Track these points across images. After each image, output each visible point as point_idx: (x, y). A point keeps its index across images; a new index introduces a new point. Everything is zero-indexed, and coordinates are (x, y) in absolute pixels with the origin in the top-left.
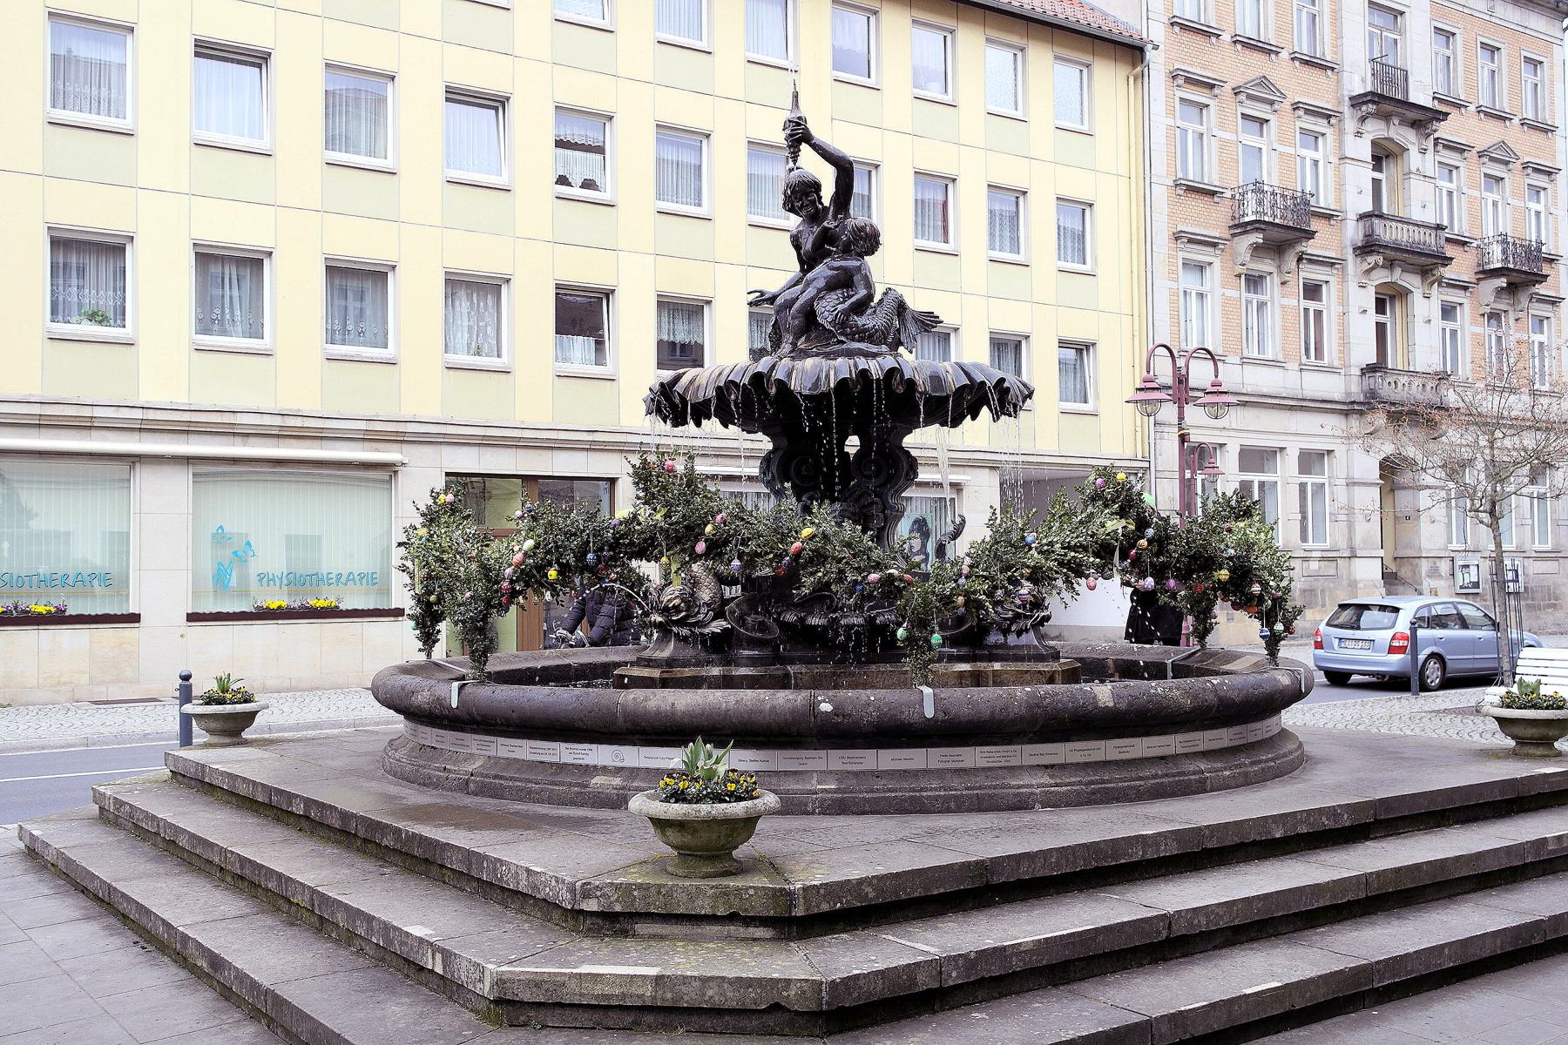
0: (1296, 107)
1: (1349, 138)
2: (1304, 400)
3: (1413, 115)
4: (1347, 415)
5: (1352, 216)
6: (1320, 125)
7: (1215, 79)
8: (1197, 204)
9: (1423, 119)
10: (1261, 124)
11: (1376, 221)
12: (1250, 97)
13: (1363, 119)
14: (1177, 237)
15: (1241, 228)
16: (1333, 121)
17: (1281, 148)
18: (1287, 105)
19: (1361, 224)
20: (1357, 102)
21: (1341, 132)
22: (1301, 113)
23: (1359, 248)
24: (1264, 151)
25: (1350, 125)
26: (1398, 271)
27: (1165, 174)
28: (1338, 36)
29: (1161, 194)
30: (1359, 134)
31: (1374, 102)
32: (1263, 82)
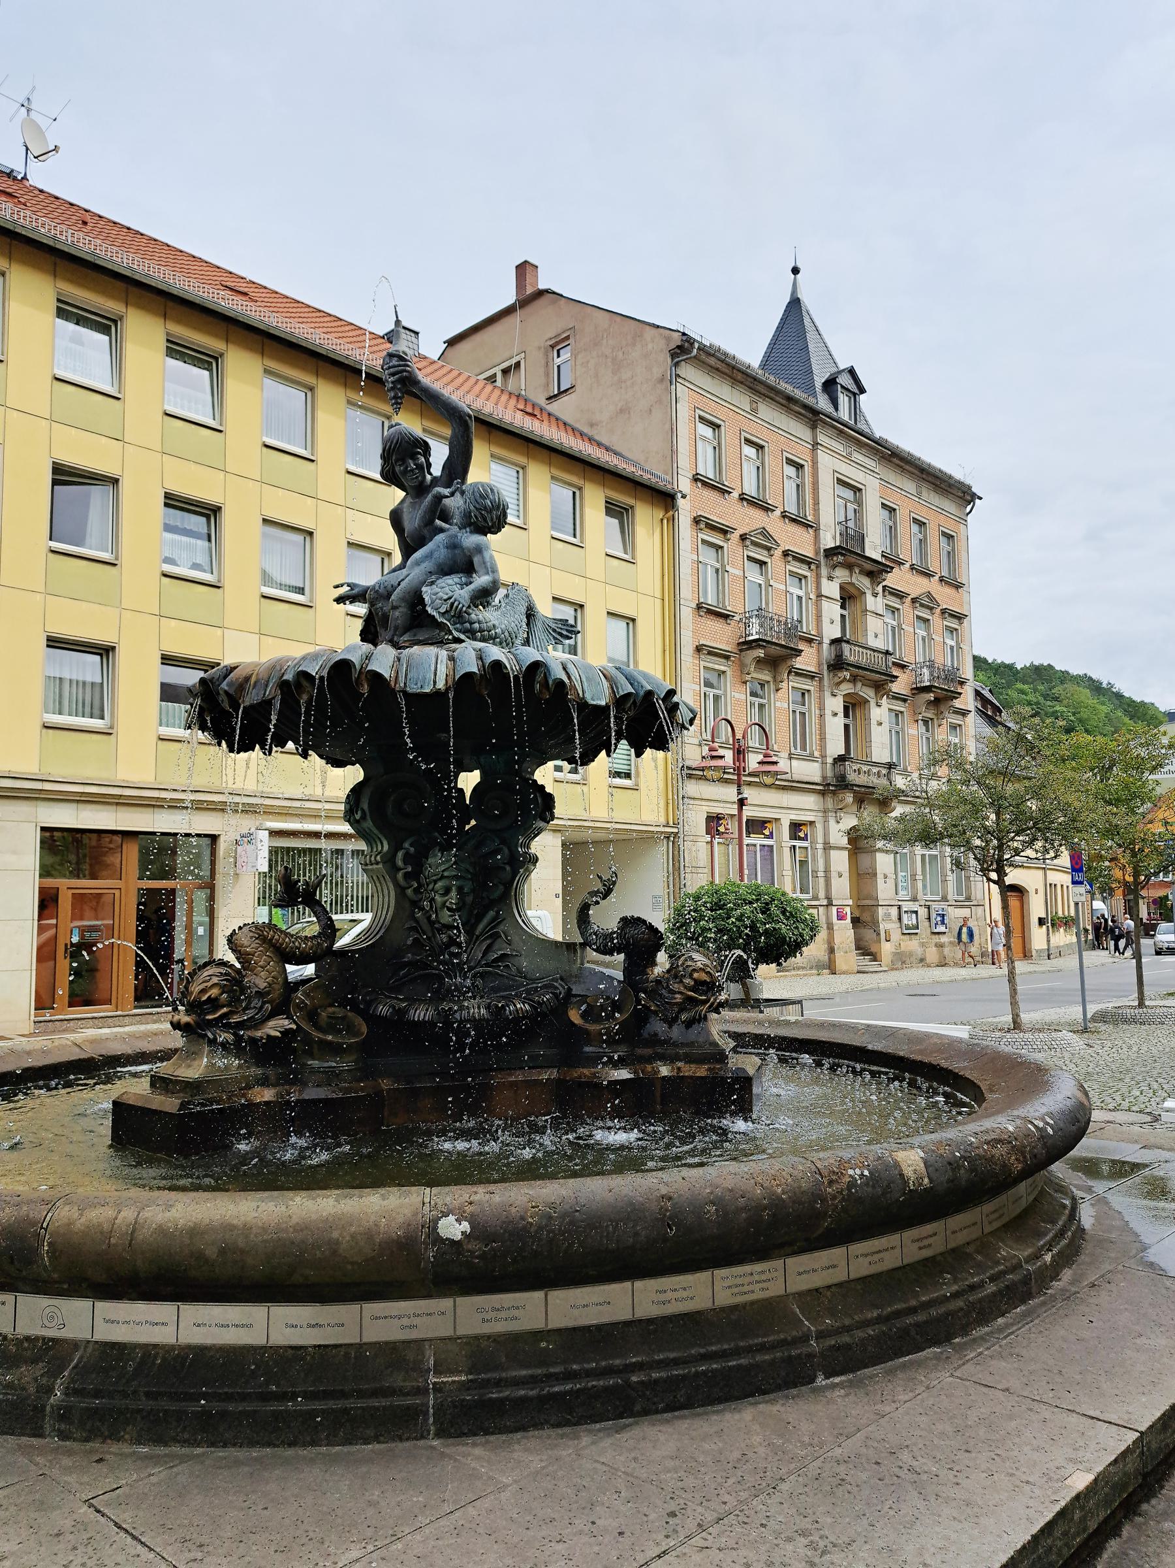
1: (824, 581)
2: (793, 781)
3: (868, 566)
4: (823, 795)
5: (826, 641)
6: (803, 570)
9: (876, 571)
10: (761, 565)
11: (844, 645)
13: (834, 567)
14: (699, 649)
15: (747, 645)
16: (813, 567)
19: (833, 647)
20: (830, 553)
21: (818, 577)
22: (790, 558)
23: (832, 665)
24: (763, 586)
25: (824, 571)
26: (859, 685)
27: (691, 598)
28: (816, 503)
29: (687, 613)
30: (830, 578)
31: (842, 555)
32: (764, 533)
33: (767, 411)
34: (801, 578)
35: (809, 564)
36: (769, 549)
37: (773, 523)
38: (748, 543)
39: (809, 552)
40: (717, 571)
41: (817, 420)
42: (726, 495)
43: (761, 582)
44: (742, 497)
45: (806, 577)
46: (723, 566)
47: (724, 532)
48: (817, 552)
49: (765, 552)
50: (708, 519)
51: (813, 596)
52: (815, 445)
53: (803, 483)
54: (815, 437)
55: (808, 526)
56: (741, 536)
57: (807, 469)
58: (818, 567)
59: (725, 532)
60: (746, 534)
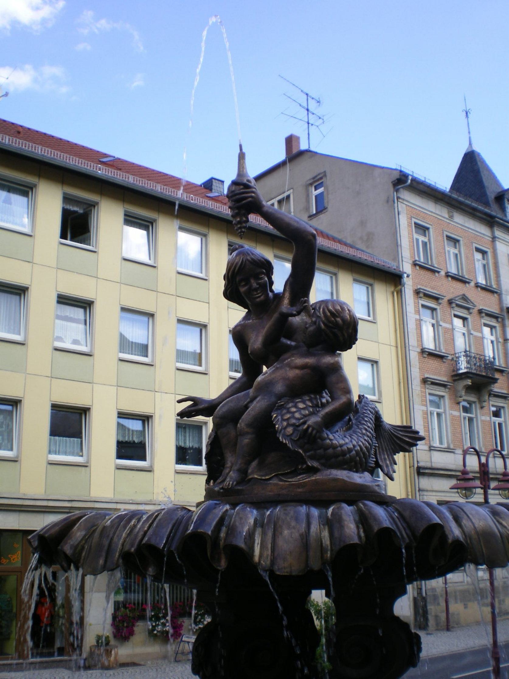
0: (480, 312)
6: (493, 322)
7: (439, 295)
8: (434, 363)
12: (458, 306)
14: (425, 381)
15: (458, 377)
16: (500, 320)
17: (475, 333)
18: (475, 311)
22: (483, 315)
28: (498, 276)
29: (414, 356)
32: (464, 298)
33: (460, 219)
34: (492, 327)
35: (496, 318)
36: (468, 309)
37: (470, 291)
38: (454, 305)
39: (494, 309)
40: (433, 325)
41: (494, 222)
42: (437, 274)
43: (465, 332)
44: (447, 275)
45: (495, 327)
46: (437, 322)
47: (436, 299)
48: (501, 309)
49: (465, 311)
50: (426, 290)
51: (501, 340)
52: (494, 238)
53: (488, 263)
54: (493, 233)
55: (493, 292)
56: (449, 301)
57: (490, 255)
58: (503, 319)
59: (436, 299)
60: (452, 299)
